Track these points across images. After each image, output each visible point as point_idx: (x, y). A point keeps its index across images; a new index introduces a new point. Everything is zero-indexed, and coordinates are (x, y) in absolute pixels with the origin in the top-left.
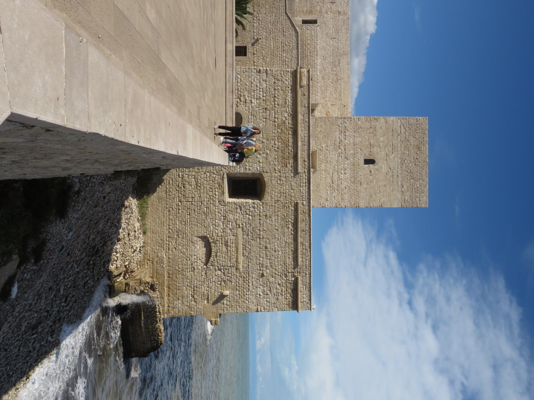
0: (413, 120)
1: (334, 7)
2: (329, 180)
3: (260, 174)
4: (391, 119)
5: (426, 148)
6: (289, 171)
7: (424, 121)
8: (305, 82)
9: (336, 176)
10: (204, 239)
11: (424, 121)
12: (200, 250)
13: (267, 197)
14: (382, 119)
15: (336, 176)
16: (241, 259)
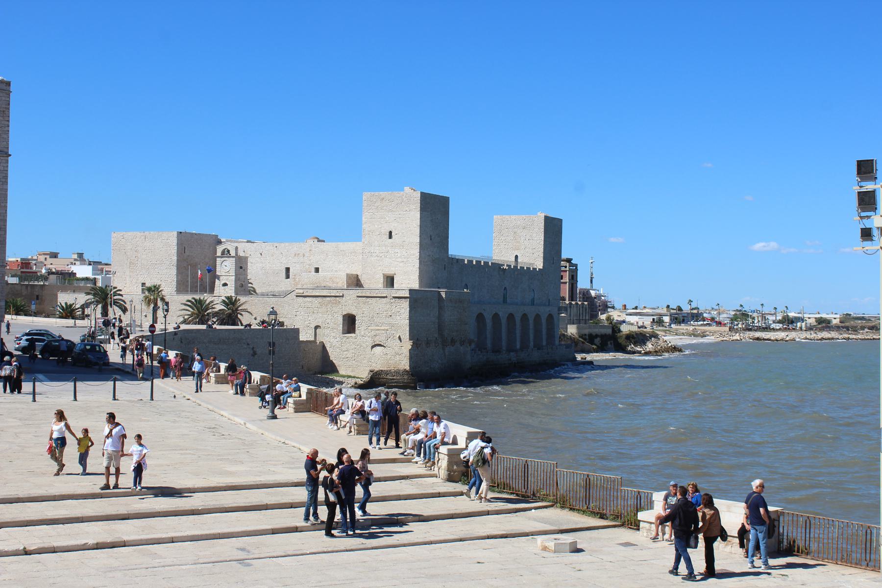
0: (365, 204)
1: (307, 255)
2: (401, 264)
3: (344, 316)
4: (364, 220)
5: (383, 194)
6: (342, 300)
7: (366, 195)
8: (301, 291)
9: (400, 260)
10: (373, 347)
11: (366, 195)
12: (378, 349)
13: (354, 313)
14: (364, 226)
15: (400, 260)
16: (383, 328)
